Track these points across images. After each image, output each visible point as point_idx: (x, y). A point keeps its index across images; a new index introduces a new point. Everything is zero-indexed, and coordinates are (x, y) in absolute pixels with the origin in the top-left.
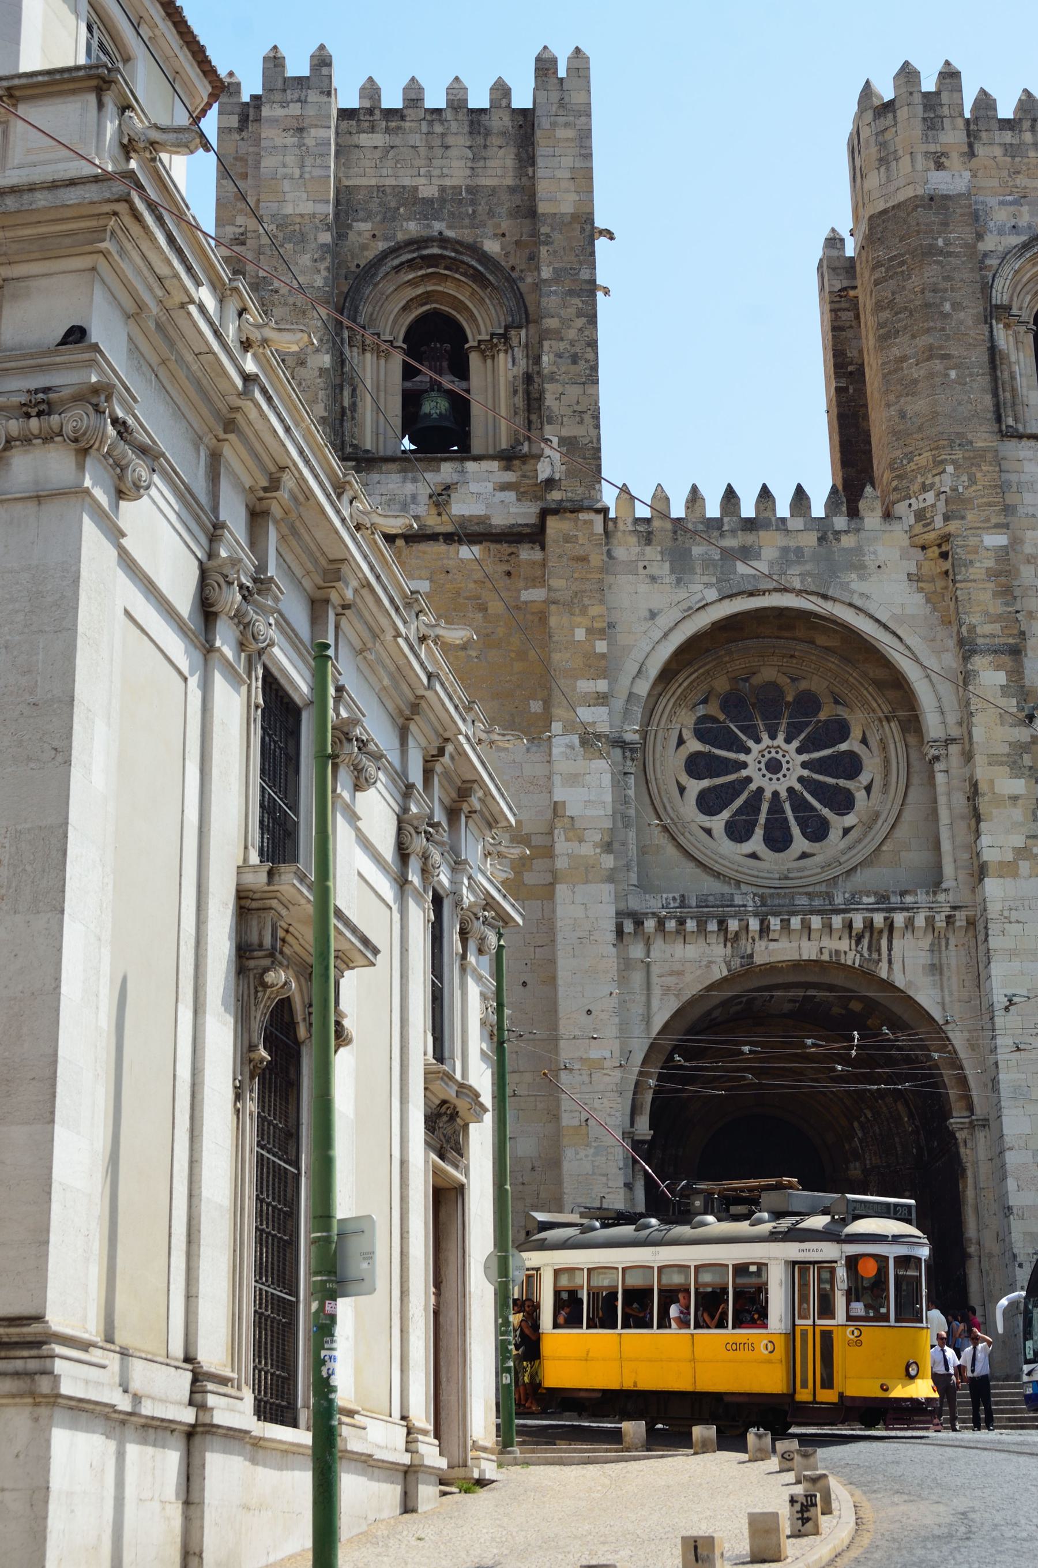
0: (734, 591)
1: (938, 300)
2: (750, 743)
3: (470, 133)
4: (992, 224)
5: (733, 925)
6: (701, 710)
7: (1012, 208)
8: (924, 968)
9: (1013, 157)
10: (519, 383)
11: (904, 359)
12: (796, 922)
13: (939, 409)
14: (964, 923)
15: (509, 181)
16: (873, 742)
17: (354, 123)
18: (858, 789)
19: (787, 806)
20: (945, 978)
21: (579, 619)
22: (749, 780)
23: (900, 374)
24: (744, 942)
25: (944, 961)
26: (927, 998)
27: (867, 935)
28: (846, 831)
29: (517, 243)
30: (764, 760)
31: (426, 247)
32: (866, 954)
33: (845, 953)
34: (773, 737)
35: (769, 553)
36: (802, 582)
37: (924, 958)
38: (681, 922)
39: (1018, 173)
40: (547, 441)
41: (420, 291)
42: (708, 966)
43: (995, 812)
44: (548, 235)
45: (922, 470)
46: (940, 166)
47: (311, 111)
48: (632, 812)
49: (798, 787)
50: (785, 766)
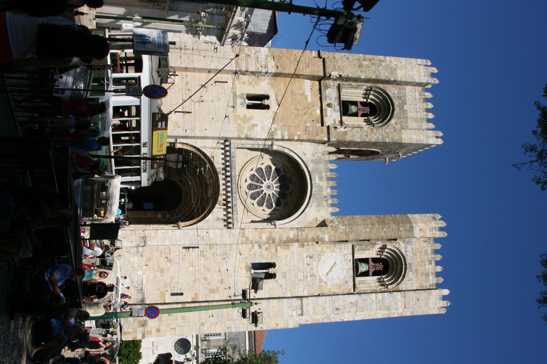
0: (311, 174)
1: (386, 227)
2: (274, 181)
3: (421, 118)
4: (407, 246)
5: (228, 169)
6: (282, 170)
7: (411, 251)
9: (424, 252)
10: (360, 126)
11: (371, 219)
13: (359, 226)
15: (410, 127)
16: (275, 212)
17: (421, 91)
19: (258, 190)
20: (215, 222)
21: (302, 133)
22: (265, 181)
23: (368, 219)
25: (220, 222)
28: (253, 204)
29: (395, 127)
30: (270, 185)
31: (392, 106)
32: (221, 202)
34: (276, 187)
35: (321, 183)
36: (314, 191)
38: (228, 157)
39: (421, 253)
40: (345, 128)
41: (382, 106)
44: (396, 131)
45: (343, 222)
46: (420, 230)
47: (423, 77)
49: (264, 193)
50: (269, 190)
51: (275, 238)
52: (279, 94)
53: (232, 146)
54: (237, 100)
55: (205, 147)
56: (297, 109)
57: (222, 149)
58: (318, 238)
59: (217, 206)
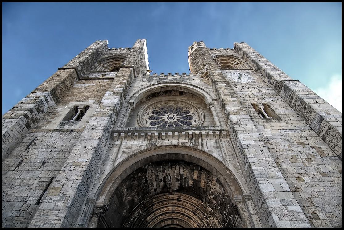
5: (150, 134)
6: (154, 109)
8: (214, 146)
12: (170, 133)
14: (226, 133)
18: (192, 121)
22: (164, 120)
24: (153, 140)
25: (221, 145)
26: (216, 154)
27: (194, 139)
32: (194, 143)
33: (187, 143)
37: (213, 144)
42: (140, 146)
43: (229, 103)
46: (200, 46)
48: (128, 115)
50: (174, 118)
51: (230, 93)
52: (77, 99)
53: (119, 129)
54: (64, 128)
55: (115, 161)
56: (98, 90)
57: (122, 141)
58: (220, 75)
59: (200, 147)
